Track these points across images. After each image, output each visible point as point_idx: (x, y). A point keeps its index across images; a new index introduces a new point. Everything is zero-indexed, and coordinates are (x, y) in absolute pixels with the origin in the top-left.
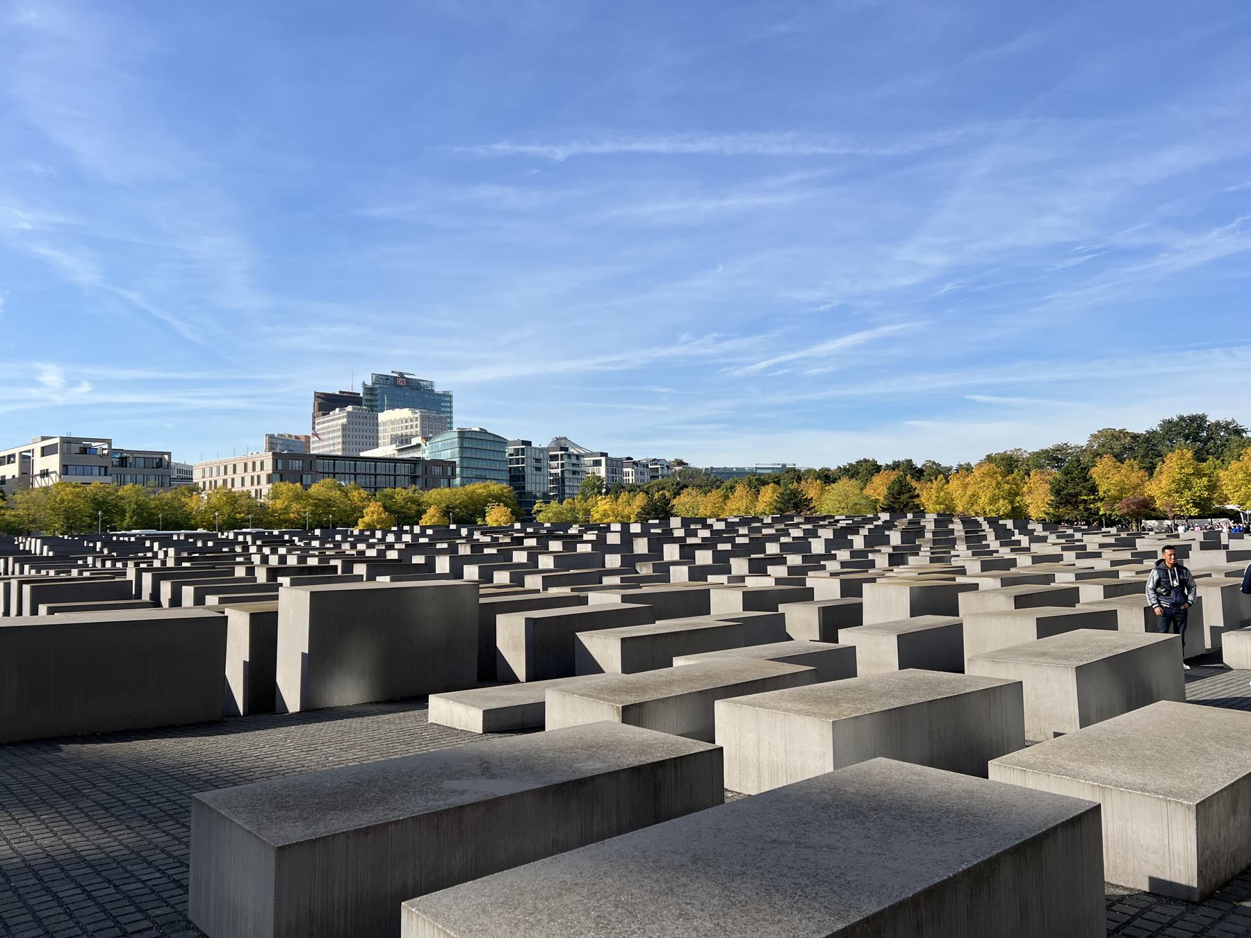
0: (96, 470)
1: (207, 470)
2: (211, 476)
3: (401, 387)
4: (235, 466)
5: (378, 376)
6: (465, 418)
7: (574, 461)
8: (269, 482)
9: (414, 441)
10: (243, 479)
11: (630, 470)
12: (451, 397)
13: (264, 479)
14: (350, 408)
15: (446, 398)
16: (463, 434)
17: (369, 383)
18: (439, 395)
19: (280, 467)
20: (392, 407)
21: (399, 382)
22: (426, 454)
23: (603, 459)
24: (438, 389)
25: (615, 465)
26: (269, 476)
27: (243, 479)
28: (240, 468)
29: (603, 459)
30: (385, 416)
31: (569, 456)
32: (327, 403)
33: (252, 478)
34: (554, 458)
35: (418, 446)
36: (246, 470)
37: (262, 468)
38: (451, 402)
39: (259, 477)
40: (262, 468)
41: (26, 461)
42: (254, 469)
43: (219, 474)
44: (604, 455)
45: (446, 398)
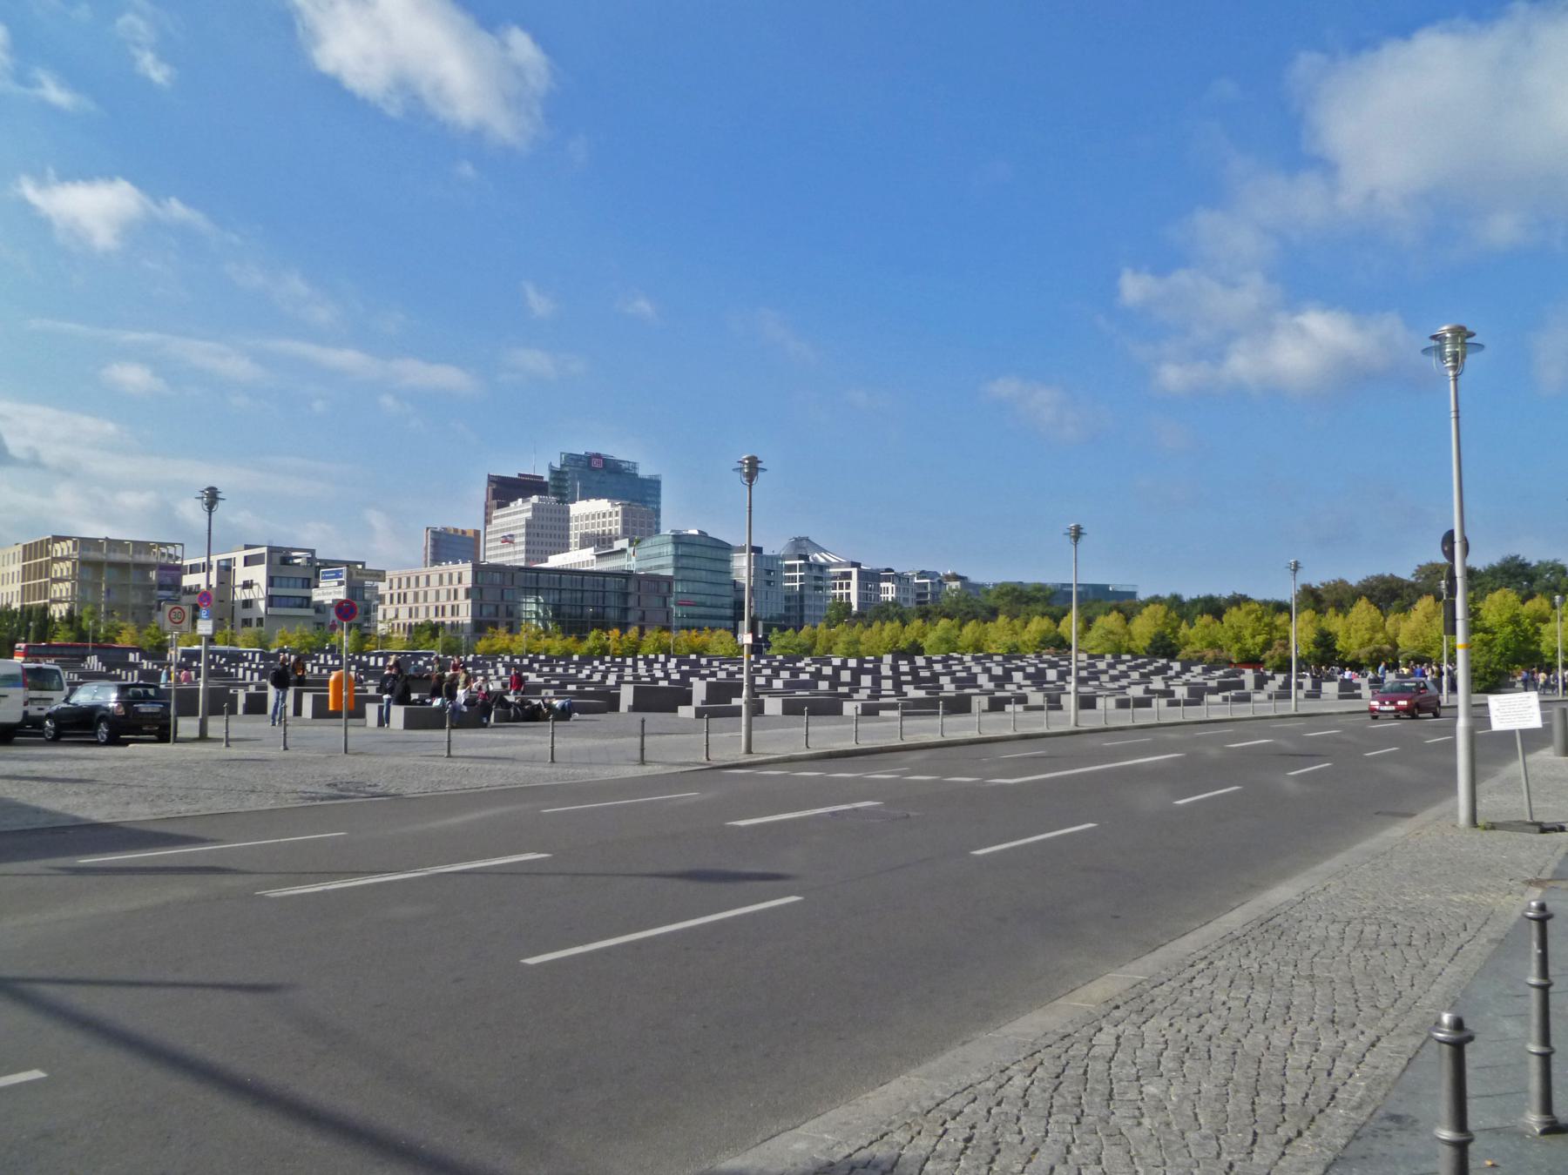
6: (678, 515)
8: (467, 597)
9: (618, 545)
11: (889, 585)
13: (462, 594)
14: (535, 499)
15: (653, 486)
16: (679, 540)
18: (643, 480)
22: (629, 563)
23: (854, 571)
25: (870, 579)
27: (438, 592)
29: (854, 571)
30: (578, 508)
34: (792, 568)
35: (623, 551)
36: (441, 582)
39: (456, 591)
41: (226, 570)
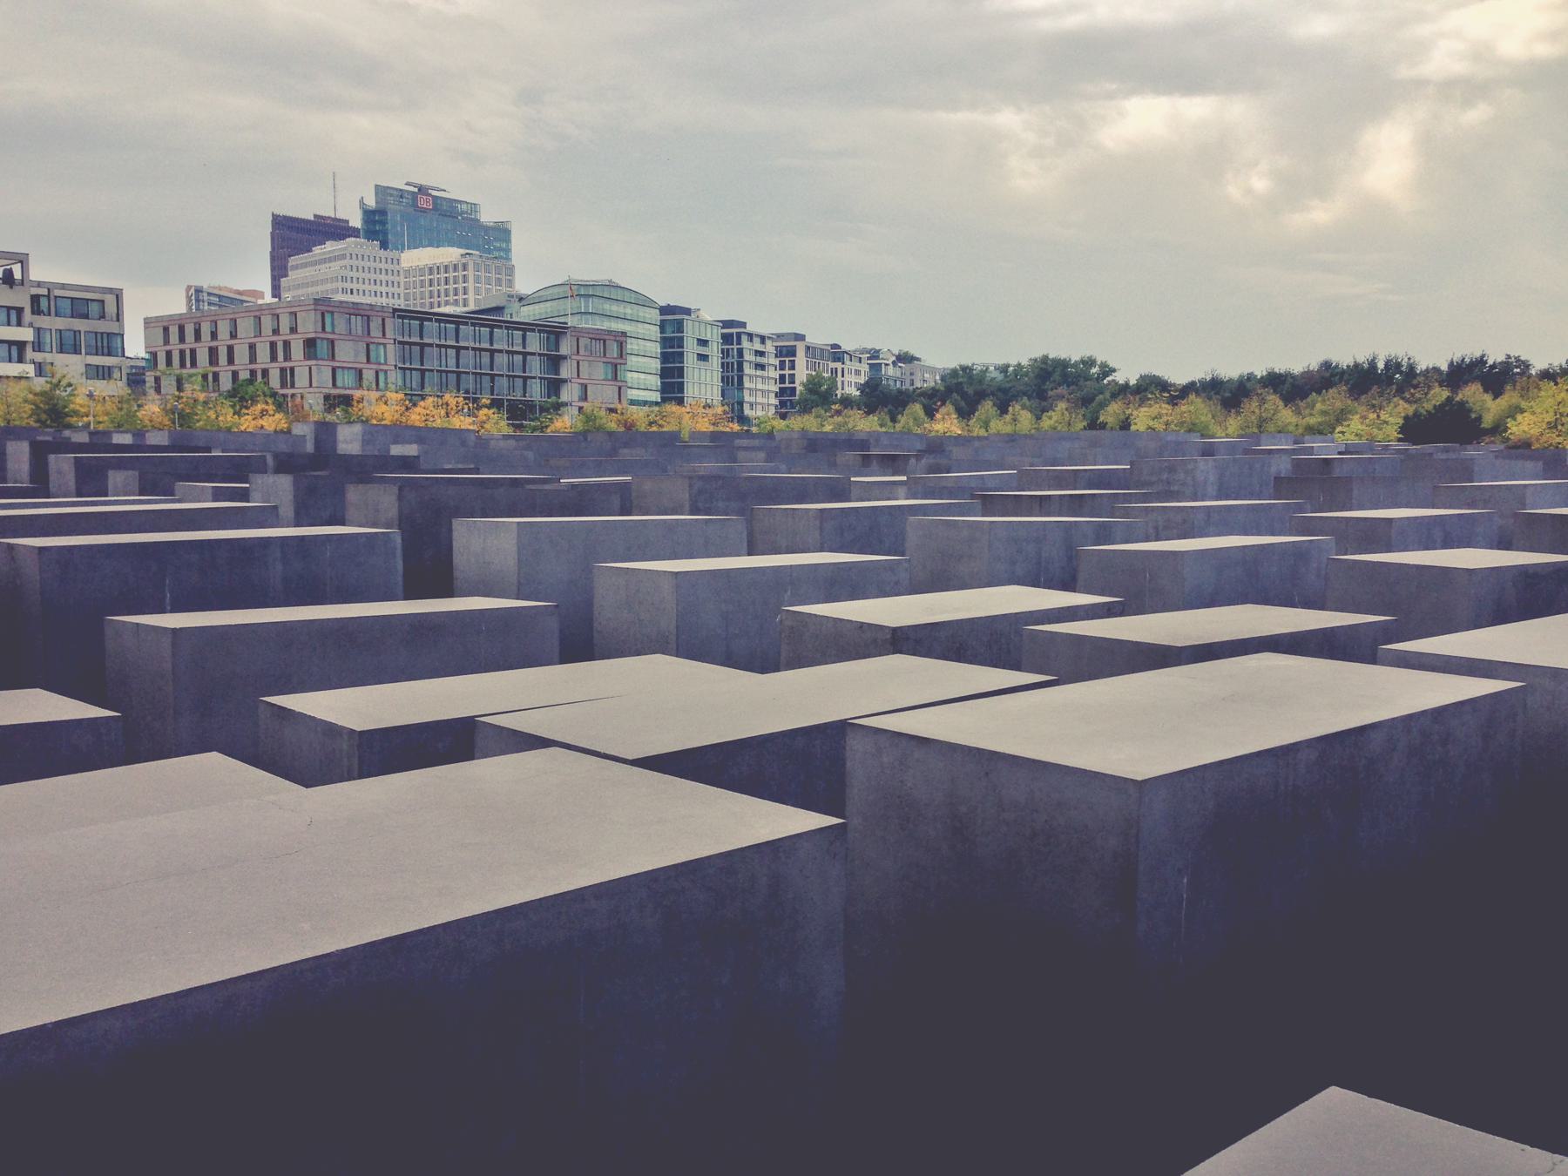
1: (174, 331)
2: (182, 339)
3: (424, 211)
5: (381, 191)
7: (758, 346)
10: (252, 347)
12: (507, 232)
17: (371, 202)
19: (328, 328)
20: (415, 244)
21: (423, 202)
24: (487, 217)
26: (310, 344)
31: (750, 336)
32: (294, 237)
33: (273, 345)
37: (293, 330)
38: (508, 241)
40: (293, 330)
42: (276, 332)
43: (198, 337)
44: (800, 337)
45: (501, 233)
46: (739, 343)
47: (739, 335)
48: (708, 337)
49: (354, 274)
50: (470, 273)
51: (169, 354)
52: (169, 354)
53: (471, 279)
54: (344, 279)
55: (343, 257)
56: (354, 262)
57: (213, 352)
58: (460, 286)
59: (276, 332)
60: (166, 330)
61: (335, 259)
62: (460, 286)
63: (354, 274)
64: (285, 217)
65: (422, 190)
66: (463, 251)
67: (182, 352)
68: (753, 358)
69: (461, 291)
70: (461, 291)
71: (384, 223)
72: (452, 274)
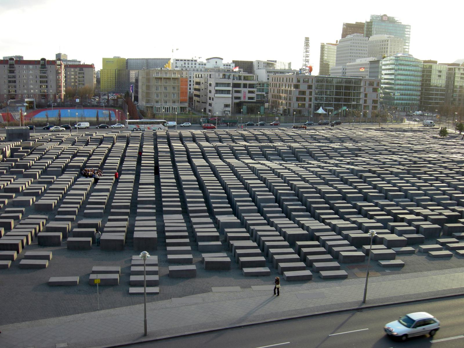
0: (227, 85)
1: (274, 78)
4: (283, 78)
17: (369, 21)
21: (384, 18)
28: (285, 79)
37: (292, 82)
40: (292, 82)
42: (289, 81)
46: (455, 71)
47: (455, 68)
48: (442, 69)
49: (354, 45)
50: (389, 43)
51: (273, 84)
52: (273, 84)
53: (389, 45)
54: (351, 46)
55: (351, 40)
56: (354, 41)
57: (280, 84)
58: (386, 47)
59: (289, 81)
60: (273, 78)
61: (349, 40)
62: (386, 47)
63: (354, 45)
64: (347, 24)
65: (385, 15)
66: (388, 36)
67: (275, 84)
68: (459, 75)
69: (386, 48)
70: (386, 48)
71: (372, 25)
72: (384, 43)
